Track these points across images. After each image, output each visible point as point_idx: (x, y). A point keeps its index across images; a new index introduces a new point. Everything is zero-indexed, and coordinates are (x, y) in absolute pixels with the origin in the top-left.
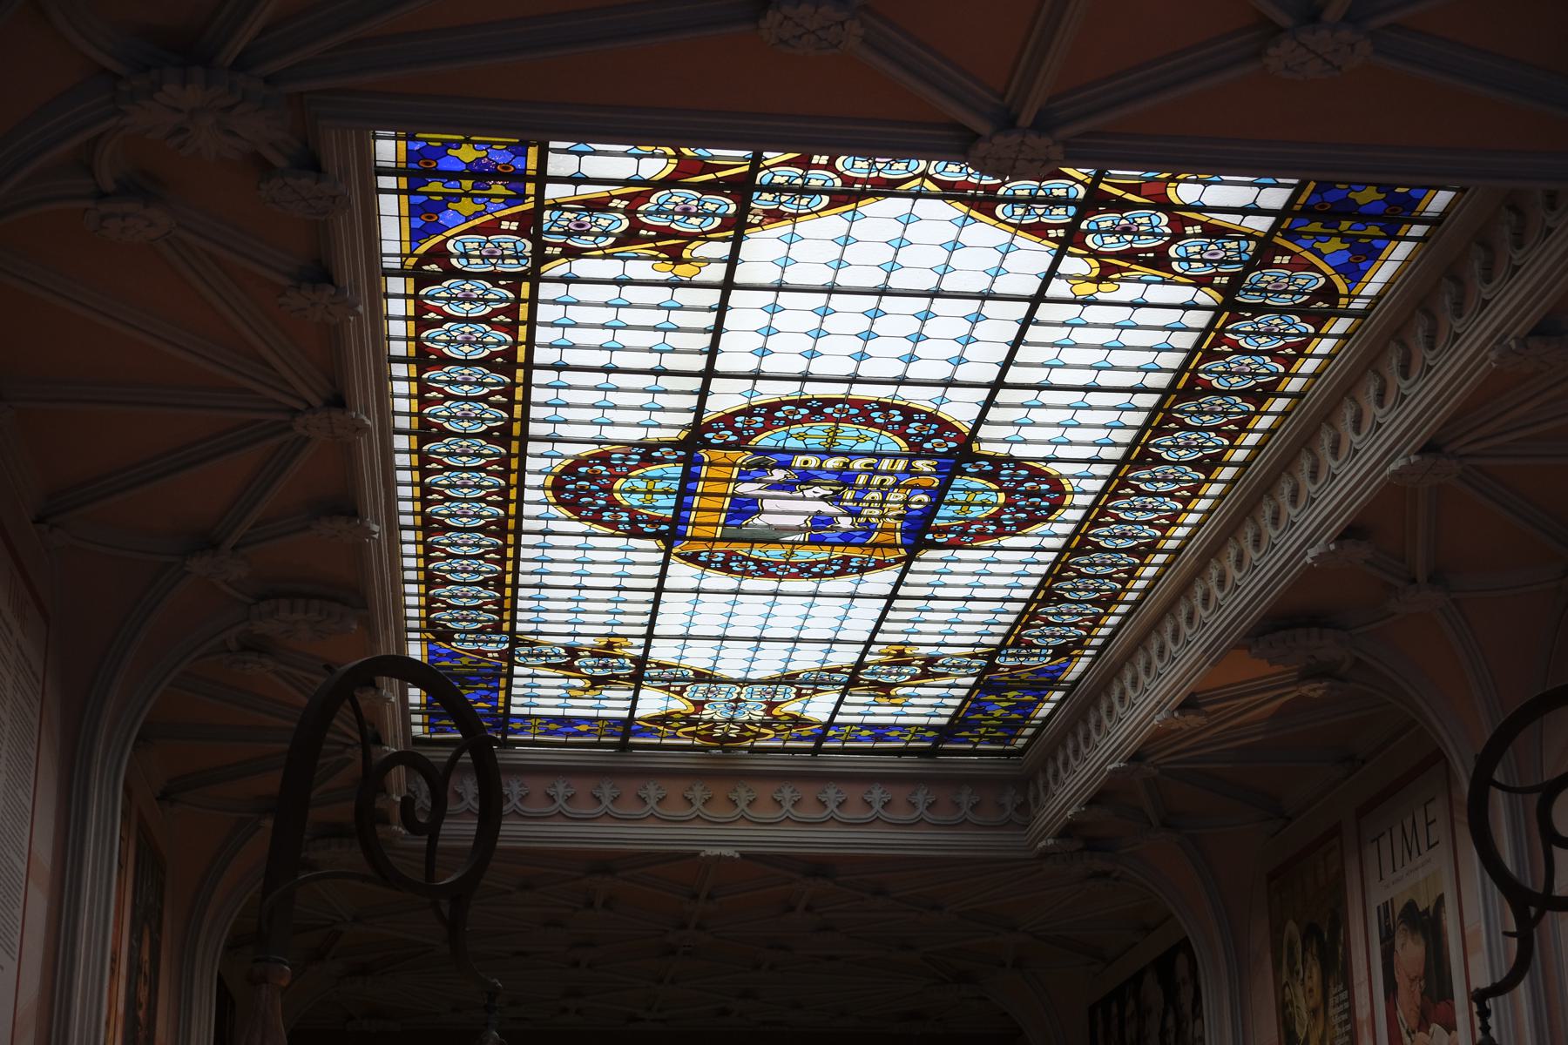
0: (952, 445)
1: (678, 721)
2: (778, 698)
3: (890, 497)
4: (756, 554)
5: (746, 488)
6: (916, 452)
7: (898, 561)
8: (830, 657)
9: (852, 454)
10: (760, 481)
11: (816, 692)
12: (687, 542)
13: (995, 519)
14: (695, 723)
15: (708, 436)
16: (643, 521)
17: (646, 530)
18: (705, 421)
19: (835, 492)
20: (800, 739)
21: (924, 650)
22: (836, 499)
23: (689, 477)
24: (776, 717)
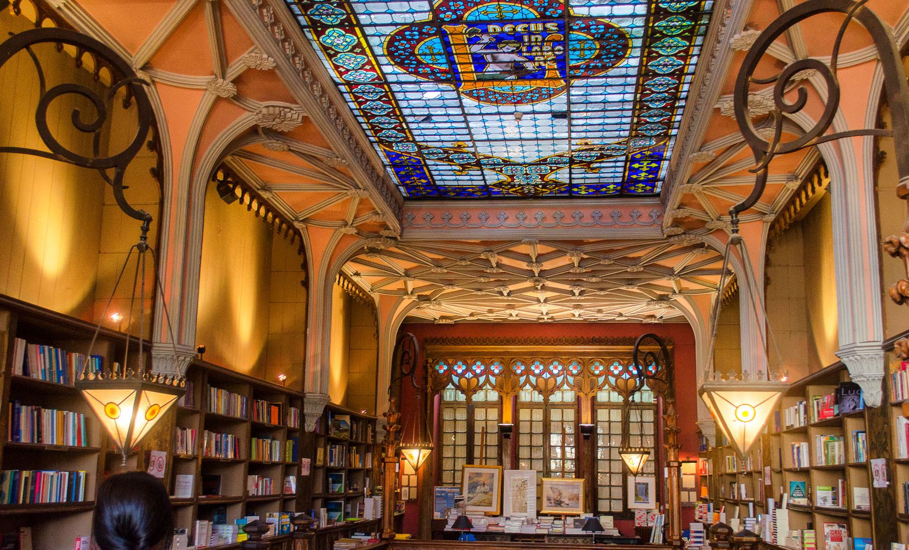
0: (560, 11)
1: (506, 185)
2: (543, 172)
3: (544, 49)
4: (497, 90)
5: (476, 49)
6: (544, 18)
7: (563, 89)
8: (556, 147)
9: (516, 22)
10: (479, 44)
11: (558, 168)
12: (463, 84)
13: (598, 57)
14: (514, 186)
15: (442, 16)
16: (439, 73)
17: (442, 78)
18: (436, 6)
19: (518, 48)
20: (562, 192)
21: (596, 142)
22: (520, 52)
23: (446, 44)
24: (547, 182)
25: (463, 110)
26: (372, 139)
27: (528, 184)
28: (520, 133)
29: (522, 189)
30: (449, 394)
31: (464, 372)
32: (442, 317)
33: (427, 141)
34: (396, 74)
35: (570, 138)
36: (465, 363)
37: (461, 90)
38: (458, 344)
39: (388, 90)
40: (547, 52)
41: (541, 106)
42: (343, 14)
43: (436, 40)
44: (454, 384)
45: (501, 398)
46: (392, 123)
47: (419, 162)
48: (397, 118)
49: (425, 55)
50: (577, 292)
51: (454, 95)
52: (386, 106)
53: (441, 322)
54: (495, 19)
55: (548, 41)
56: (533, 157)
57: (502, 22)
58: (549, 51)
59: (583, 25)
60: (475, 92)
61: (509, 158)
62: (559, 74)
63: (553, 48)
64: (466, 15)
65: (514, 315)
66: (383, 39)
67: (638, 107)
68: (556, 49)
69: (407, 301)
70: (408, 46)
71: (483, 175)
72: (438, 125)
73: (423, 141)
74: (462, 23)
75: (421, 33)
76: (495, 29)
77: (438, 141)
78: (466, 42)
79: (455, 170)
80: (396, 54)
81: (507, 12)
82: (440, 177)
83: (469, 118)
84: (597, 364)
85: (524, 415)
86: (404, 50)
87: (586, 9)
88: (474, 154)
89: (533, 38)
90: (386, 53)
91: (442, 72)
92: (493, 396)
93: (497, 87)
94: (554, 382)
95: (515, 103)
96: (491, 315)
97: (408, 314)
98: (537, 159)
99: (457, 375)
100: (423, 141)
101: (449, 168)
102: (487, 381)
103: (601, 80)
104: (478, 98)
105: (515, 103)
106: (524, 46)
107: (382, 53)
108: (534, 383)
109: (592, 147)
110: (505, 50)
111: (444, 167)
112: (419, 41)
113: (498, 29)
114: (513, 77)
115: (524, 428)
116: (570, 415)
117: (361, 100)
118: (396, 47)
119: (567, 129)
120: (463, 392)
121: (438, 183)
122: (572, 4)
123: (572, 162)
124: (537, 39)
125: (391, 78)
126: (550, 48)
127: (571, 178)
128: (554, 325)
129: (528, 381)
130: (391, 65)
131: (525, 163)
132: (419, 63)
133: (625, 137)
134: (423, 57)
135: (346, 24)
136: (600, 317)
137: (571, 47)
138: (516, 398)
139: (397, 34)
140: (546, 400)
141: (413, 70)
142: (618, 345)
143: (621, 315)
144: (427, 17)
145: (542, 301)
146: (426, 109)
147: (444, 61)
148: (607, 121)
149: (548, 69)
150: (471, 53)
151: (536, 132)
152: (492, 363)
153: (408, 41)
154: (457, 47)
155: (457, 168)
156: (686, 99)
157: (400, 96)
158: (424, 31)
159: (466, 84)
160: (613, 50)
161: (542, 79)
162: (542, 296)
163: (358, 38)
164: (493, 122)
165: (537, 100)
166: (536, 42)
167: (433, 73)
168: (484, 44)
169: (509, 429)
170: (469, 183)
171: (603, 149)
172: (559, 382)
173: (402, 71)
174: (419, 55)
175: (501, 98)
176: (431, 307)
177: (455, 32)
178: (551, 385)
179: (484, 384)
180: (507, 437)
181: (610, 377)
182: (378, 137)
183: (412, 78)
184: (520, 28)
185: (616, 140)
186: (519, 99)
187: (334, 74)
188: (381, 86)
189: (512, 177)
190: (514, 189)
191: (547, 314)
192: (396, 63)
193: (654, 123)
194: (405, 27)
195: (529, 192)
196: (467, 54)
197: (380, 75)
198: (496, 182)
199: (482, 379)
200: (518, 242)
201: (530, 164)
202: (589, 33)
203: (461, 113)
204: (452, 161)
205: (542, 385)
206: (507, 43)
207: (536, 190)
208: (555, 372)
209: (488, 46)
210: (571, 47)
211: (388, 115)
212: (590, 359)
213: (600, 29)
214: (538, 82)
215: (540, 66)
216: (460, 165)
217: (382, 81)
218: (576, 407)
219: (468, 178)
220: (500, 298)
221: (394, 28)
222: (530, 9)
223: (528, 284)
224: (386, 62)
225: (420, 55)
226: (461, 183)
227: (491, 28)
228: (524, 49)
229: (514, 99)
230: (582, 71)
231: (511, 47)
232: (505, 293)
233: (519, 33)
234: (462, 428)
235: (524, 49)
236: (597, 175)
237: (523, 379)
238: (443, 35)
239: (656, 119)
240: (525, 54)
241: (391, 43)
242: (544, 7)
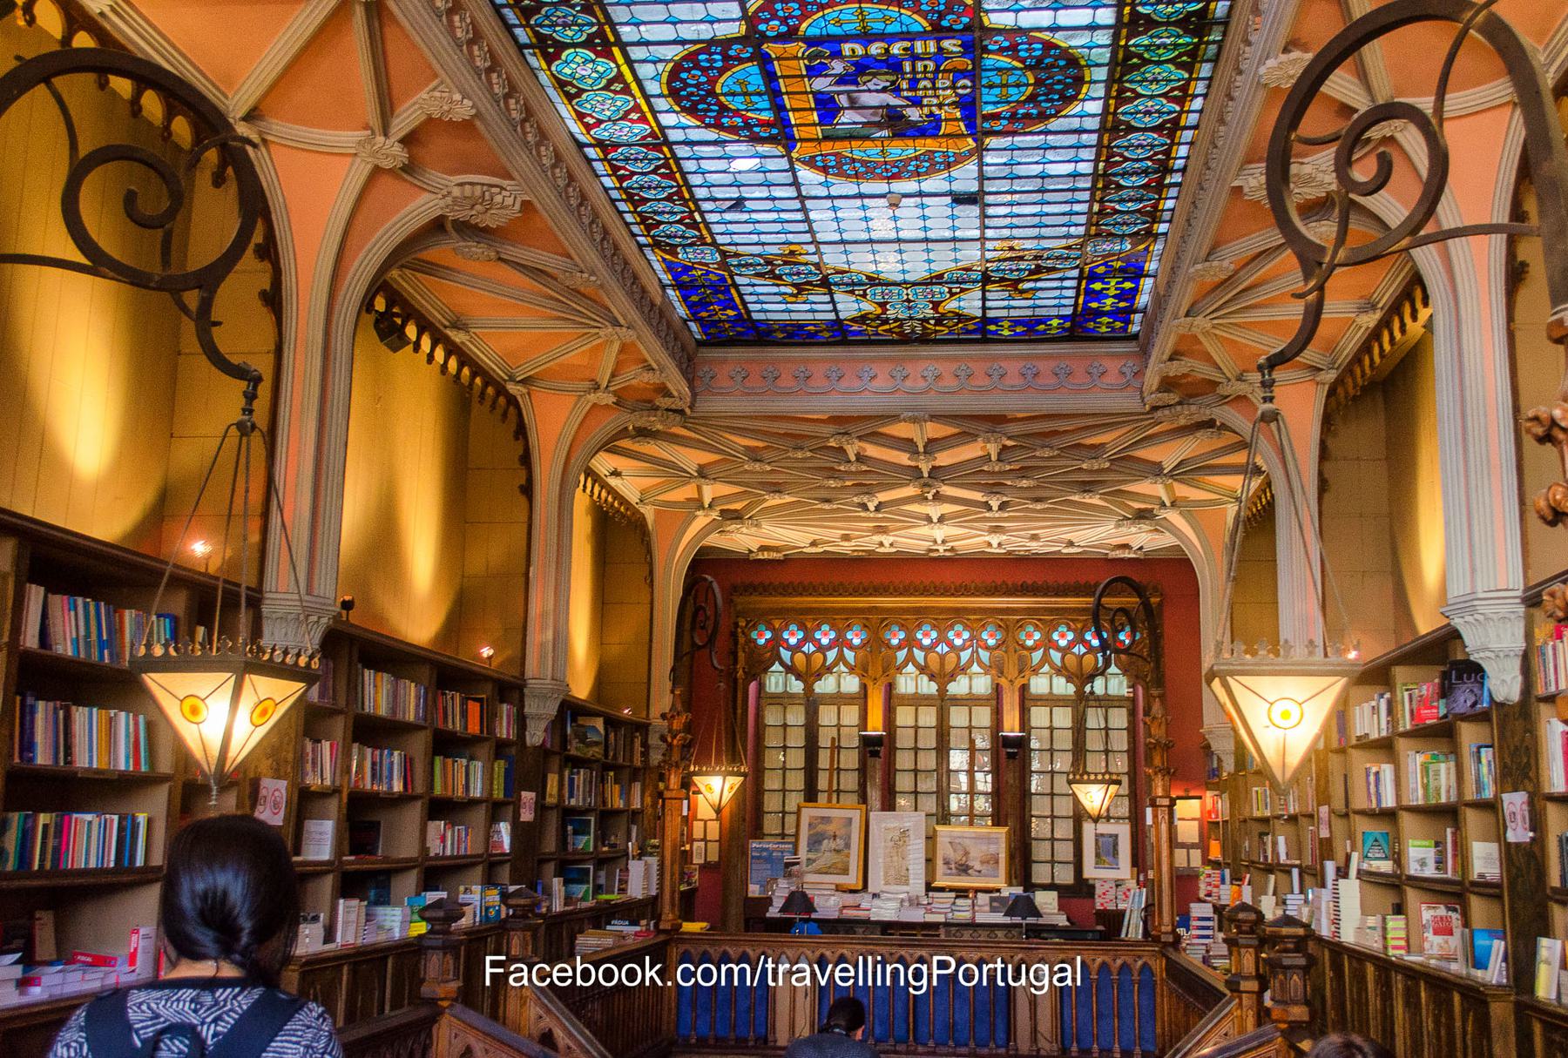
0: (965, 20)
1: (872, 320)
2: (937, 298)
3: (939, 84)
4: (857, 155)
5: (821, 84)
6: (938, 31)
7: (971, 153)
9: (890, 38)
10: (826, 76)
11: (963, 290)
12: (799, 145)
13: (1032, 98)
14: (886, 321)
15: (762, 27)
16: (757, 126)
17: (762, 134)
18: (752, 10)
19: (893, 83)
21: (1028, 244)
22: (896, 91)
23: (770, 77)
24: (943, 314)
25: (799, 191)
26: (642, 240)
27: (911, 318)
28: (897, 230)
29: (901, 326)
30: (775, 681)
31: (801, 643)
32: (763, 548)
33: (737, 244)
34: (684, 128)
35: (983, 239)
36: (802, 627)
37: (795, 155)
38: (790, 595)
39: (669, 156)
40: (944, 89)
41: (933, 184)
42: (592, 25)
43: (753, 69)
44: (782, 663)
45: (864, 687)
46: (675, 213)
47: (723, 279)
48: (685, 204)
49: (734, 94)
50: (995, 504)
51: (784, 164)
52: (665, 183)
53: (761, 557)
54: (854, 32)
55: (945, 71)
56: (919, 271)
57: (866, 37)
58: (947, 88)
59: (1006, 44)
60: (819, 158)
61: (878, 273)
62: (963, 128)
63: (954, 83)
64: (804, 25)
65: (887, 544)
66: (660, 67)
67: (1100, 185)
68: (959, 85)
69: (702, 520)
70: (703, 79)
71: (833, 301)
72: (755, 216)
73: (729, 244)
74: (797, 40)
75: (726, 58)
76: (853, 51)
77: (756, 244)
78: (804, 73)
79: (785, 294)
80: (683, 93)
81: (875, 20)
82: (758, 307)
83: (809, 204)
84: (1030, 629)
85: (904, 716)
86: (697, 86)
87: (1012, 15)
88: (817, 265)
89: (920, 66)
90: (666, 92)
91: (762, 124)
92: (851, 684)
93: (858, 150)
94: (955, 660)
95: (889, 178)
96: (846, 544)
97: (704, 543)
98: (926, 275)
99: (789, 648)
100: (729, 244)
101: (775, 289)
102: (841, 658)
103: (1036, 138)
104: (825, 170)
105: (889, 178)
106: (903, 79)
107: (659, 92)
108: (922, 662)
109: (1021, 254)
110: (871, 86)
111: (766, 288)
112: (722, 71)
113: (860, 50)
114: (885, 133)
115: (904, 739)
116: (983, 716)
117: (622, 172)
118: (684, 81)
119: (977, 223)
120: (799, 677)
121: (755, 316)
122: (986, 6)
123: (986, 279)
124: (925, 67)
125: (674, 136)
126: (948, 83)
127: (984, 308)
128: (955, 561)
129: (910, 658)
130: (674, 112)
131: (905, 282)
132: (723, 108)
133: (1078, 237)
134: (730, 98)
135: (597, 41)
136: (1035, 547)
137: (984, 82)
138: (890, 687)
139: (684, 58)
140: (942, 691)
141: (712, 121)
142: (1066, 595)
143: (1071, 544)
144: (736, 29)
145: (935, 520)
146: (735, 189)
147: (766, 105)
148: (1047, 209)
149: (946, 120)
150: (812, 92)
151: (925, 229)
152: (849, 627)
153: (704, 70)
154: (788, 81)
155: (789, 290)
156: (1183, 170)
157: (689, 166)
158: (732, 53)
159: (805, 144)
160: (1057, 87)
161: (935, 136)
162: (935, 511)
163: (618, 66)
164: (849, 211)
165: (926, 173)
166: (925, 72)
167: (747, 125)
168: (835, 75)
169: (878, 741)
170: (810, 316)
171: (1040, 258)
172: (964, 660)
173: (693, 122)
174: (722, 94)
175: (863, 169)
176: (744, 530)
177: (785, 55)
178: (950, 666)
179: (835, 664)
180: (875, 754)
181: (1052, 651)
182: (653, 237)
183: (711, 135)
184: (896, 49)
185: (1063, 243)
186: (895, 170)
187: (576, 128)
188: (657, 148)
189: (883, 305)
190: (887, 327)
191: (944, 542)
192: (684, 109)
193: (1127, 212)
194: (698, 46)
195: (913, 331)
196: (806, 93)
197: (656, 129)
198: (855, 314)
199: (832, 655)
200: (894, 418)
201: (915, 284)
202: (1016, 57)
203: (795, 195)
204: (779, 277)
205: (934, 666)
206: (874, 75)
207: (925, 328)
208: (958, 642)
209: (842, 80)
210: (984, 82)
211: (669, 198)
212: (1018, 621)
213: (1034, 50)
214: (929, 141)
215: (931, 114)
216: (794, 285)
217: (659, 141)
218: (994, 702)
219: (807, 307)
220: (863, 514)
221: (679, 48)
222: (915, 16)
223: (911, 491)
224: (667, 107)
225: (725, 95)
226: (795, 316)
227: (846, 48)
228: (905, 85)
229: (887, 170)
230: (1005, 122)
231: (881, 82)
232: (871, 506)
233: (894, 56)
234: (797, 739)
235: (905, 85)
236: (1030, 303)
237: (901, 655)
238: (765, 61)
239: (1131, 206)
240: (905, 94)
241: (674, 75)
242: (938, 12)
